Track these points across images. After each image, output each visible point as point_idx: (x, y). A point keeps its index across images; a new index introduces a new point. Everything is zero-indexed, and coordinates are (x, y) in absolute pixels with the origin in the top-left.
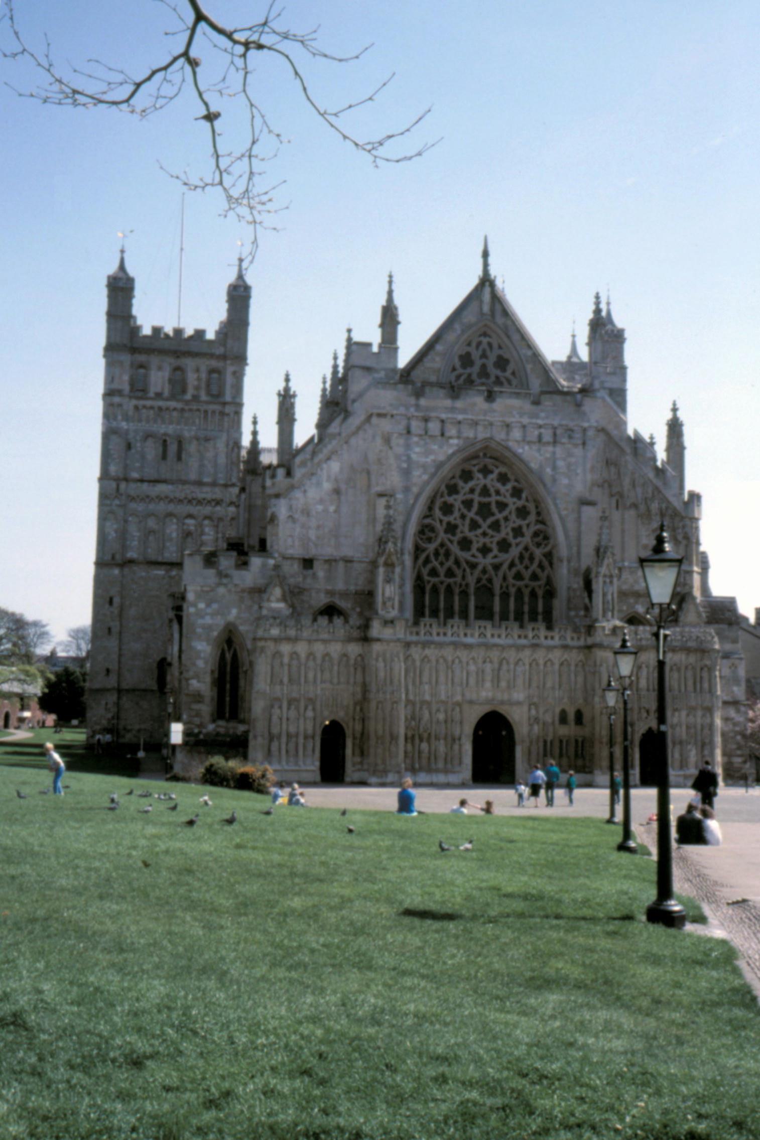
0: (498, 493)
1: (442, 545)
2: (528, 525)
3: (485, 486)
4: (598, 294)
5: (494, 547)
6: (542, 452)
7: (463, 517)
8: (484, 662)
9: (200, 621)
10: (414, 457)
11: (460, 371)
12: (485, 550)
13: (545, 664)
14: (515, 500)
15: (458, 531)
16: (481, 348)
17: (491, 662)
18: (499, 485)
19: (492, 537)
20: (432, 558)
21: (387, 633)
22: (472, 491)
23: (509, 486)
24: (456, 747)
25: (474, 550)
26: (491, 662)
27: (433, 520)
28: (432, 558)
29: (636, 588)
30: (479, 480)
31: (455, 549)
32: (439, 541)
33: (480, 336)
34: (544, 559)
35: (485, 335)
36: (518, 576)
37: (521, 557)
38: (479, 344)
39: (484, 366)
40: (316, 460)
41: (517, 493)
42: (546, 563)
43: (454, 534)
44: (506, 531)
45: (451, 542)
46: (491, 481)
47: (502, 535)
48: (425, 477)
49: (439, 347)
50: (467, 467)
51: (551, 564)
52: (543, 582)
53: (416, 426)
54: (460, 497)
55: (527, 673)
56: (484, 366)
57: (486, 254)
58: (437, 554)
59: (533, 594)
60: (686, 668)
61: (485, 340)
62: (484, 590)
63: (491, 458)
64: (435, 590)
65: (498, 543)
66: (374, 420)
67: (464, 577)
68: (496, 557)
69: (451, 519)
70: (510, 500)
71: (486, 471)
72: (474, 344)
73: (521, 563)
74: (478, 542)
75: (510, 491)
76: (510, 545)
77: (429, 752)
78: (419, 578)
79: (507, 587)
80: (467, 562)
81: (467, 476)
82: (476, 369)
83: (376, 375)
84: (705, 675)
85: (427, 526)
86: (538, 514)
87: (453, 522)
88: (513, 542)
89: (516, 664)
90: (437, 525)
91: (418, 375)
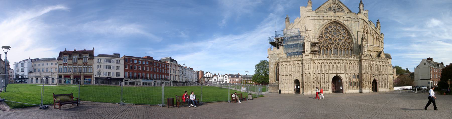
2: (346, 36)
5: (337, 40)
8: (334, 63)
12: (336, 41)
19: (337, 38)
24: (327, 85)
25: (333, 41)
26: (336, 63)
31: (328, 41)
32: (324, 39)
43: (328, 38)
45: (327, 40)
47: (340, 38)
48: (319, 27)
52: (350, 47)
54: (329, 31)
68: (338, 42)
69: (327, 35)
79: (341, 48)
80: (331, 43)
90: (323, 36)
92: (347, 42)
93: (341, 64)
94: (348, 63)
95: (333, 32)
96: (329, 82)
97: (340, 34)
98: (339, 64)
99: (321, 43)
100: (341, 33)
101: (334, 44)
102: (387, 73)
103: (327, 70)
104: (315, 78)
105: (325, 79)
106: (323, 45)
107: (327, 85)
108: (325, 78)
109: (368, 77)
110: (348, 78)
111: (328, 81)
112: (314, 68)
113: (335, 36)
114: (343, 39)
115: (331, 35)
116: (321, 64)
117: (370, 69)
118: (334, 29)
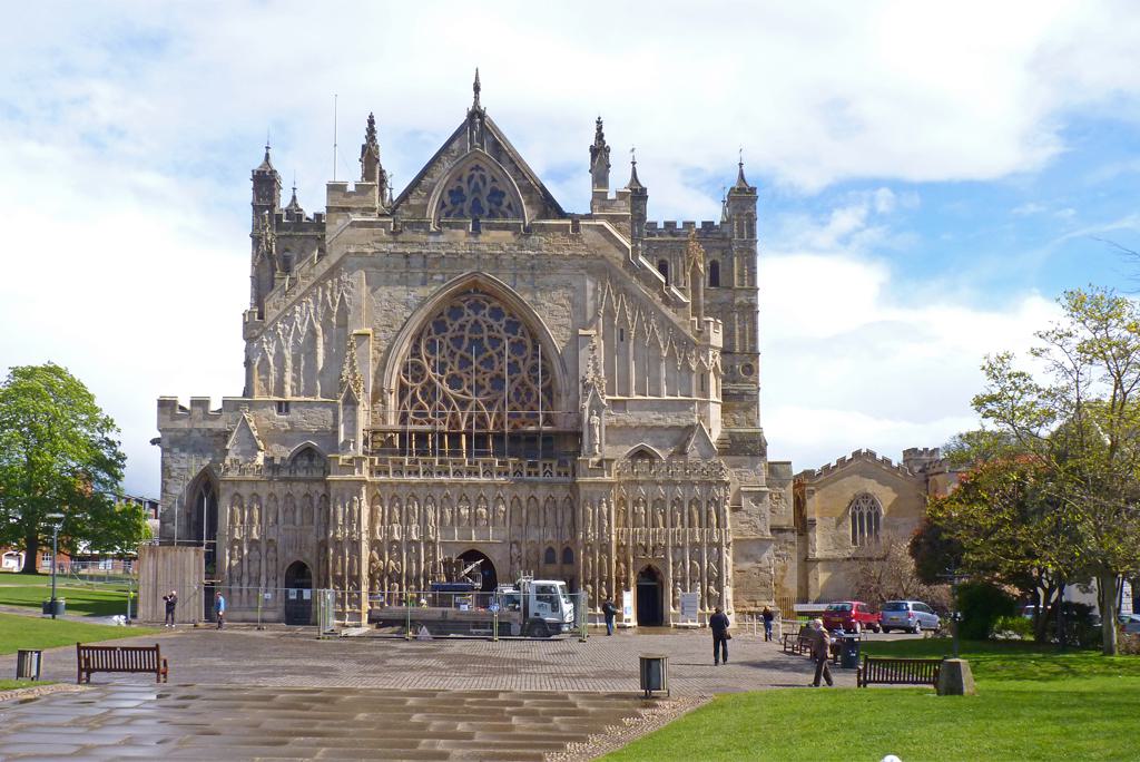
0: (490, 327)
2: (525, 360)
3: (476, 322)
5: (487, 384)
6: (536, 284)
7: (453, 354)
9: (175, 465)
11: (449, 207)
13: (528, 501)
14: (510, 335)
16: (473, 182)
18: (491, 321)
22: (462, 327)
23: (503, 322)
26: (467, 500)
30: (469, 316)
33: (472, 169)
35: (477, 168)
38: (472, 177)
41: (512, 326)
45: (441, 380)
46: (484, 316)
47: (496, 370)
50: (457, 303)
54: (449, 335)
57: (477, 88)
58: (423, 393)
61: (477, 174)
68: (489, 393)
70: (504, 335)
71: (477, 307)
72: (465, 179)
73: (517, 400)
80: (457, 400)
81: (456, 312)
82: (467, 206)
92: (528, 389)
94: (524, 499)
95: (466, 341)
97: (498, 349)
101: (469, 401)
102: (716, 540)
106: (422, 407)
108: (423, 560)
110: (520, 562)
116: (404, 501)
117: (626, 521)
118: (472, 321)
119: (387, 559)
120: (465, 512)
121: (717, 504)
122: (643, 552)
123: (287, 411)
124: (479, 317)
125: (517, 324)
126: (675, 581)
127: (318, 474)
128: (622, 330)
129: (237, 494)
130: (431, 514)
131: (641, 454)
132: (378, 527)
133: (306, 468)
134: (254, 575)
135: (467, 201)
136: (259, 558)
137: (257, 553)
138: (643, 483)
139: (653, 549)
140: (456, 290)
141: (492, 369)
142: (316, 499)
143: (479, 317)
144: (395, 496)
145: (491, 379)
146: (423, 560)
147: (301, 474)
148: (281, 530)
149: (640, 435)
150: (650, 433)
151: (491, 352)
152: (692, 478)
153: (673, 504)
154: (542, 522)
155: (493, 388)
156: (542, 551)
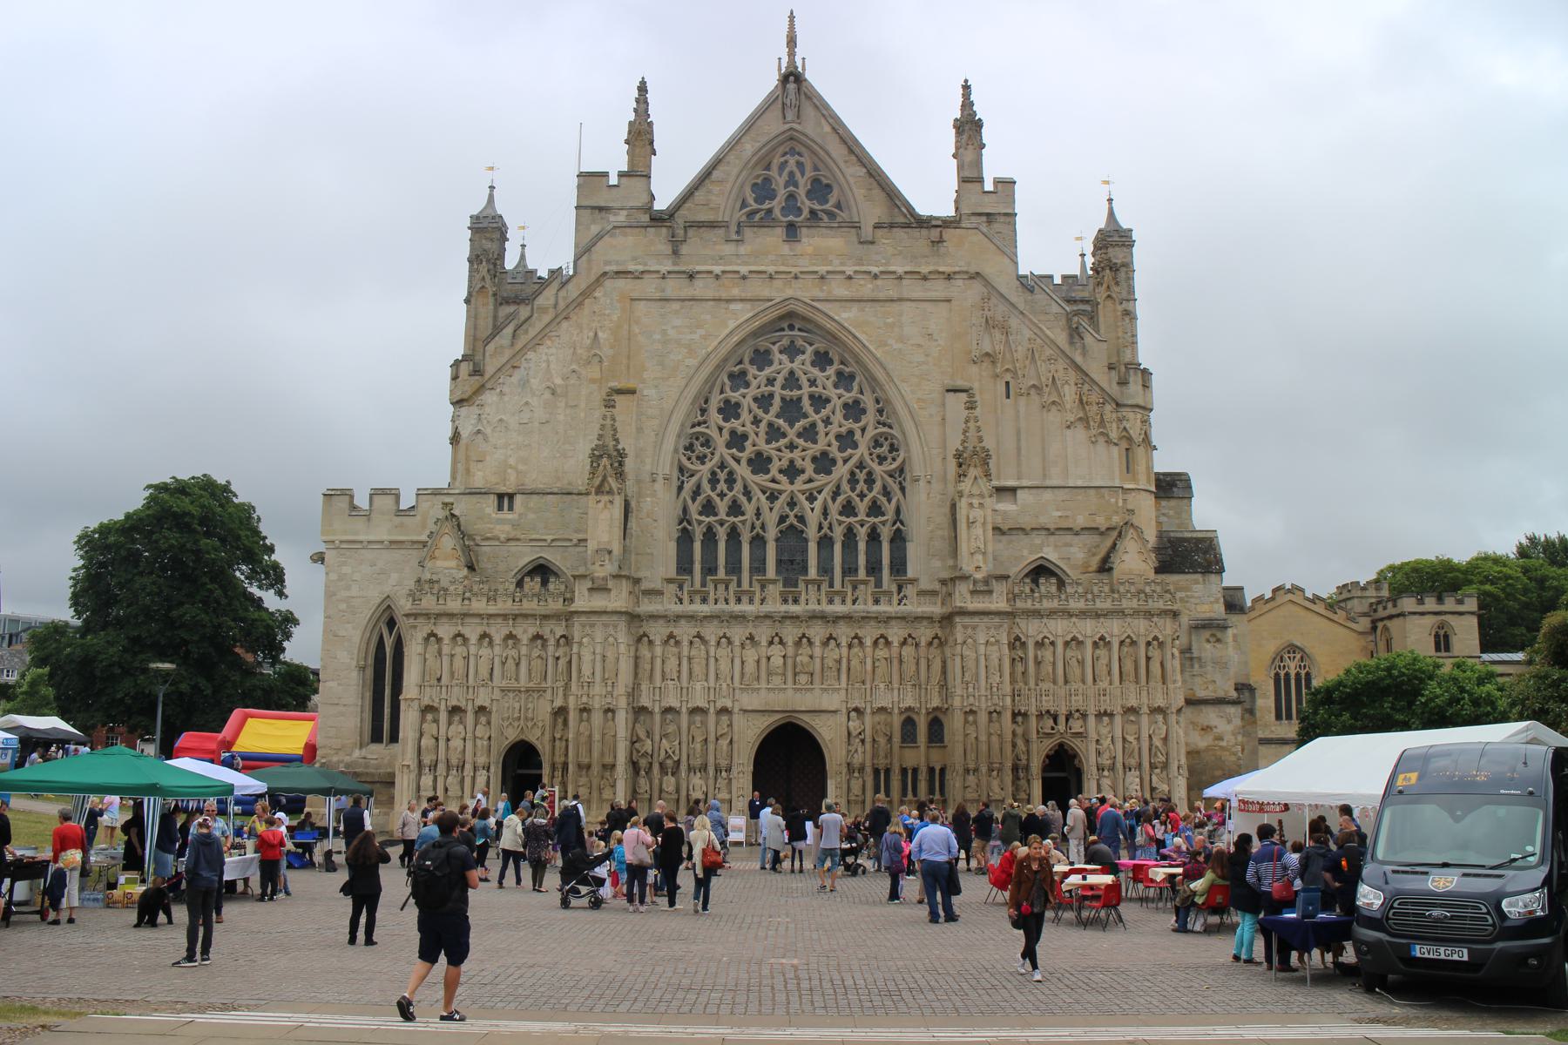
0: (813, 383)
1: (722, 466)
2: (863, 430)
3: (792, 373)
4: (966, 81)
8: (771, 643)
10: (672, 333)
12: (792, 472)
13: (876, 643)
15: (748, 444)
17: (781, 642)
18: (816, 372)
20: (706, 486)
21: (599, 602)
24: (721, 783)
25: (774, 472)
26: (781, 642)
27: (707, 427)
28: (706, 486)
29: (1043, 520)
30: (781, 364)
31: (743, 471)
32: (716, 458)
34: (890, 480)
35: (792, 152)
36: (848, 509)
37: (853, 481)
39: (791, 197)
40: (519, 346)
41: (844, 380)
42: (896, 488)
43: (742, 449)
44: (825, 441)
45: (738, 461)
46: (802, 364)
47: (821, 446)
49: (716, 175)
50: (763, 344)
51: (903, 489)
52: (890, 516)
53: (673, 287)
55: (844, 661)
56: (791, 197)
57: (792, 42)
58: (714, 481)
59: (874, 536)
60: (1122, 643)
61: (792, 161)
62: (792, 534)
63: (800, 330)
64: (710, 535)
65: (814, 459)
66: (608, 283)
67: (758, 514)
68: (810, 481)
71: (792, 351)
73: (853, 490)
74: (780, 460)
75: (833, 378)
76: (834, 462)
77: (678, 791)
78: (684, 517)
79: (830, 528)
82: (777, 204)
83: (612, 218)
84: (1155, 653)
85: (697, 436)
86: (880, 411)
87: (740, 429)
88: (839, 456)
89: (825, 644)
90: (714, 433)
91: (684, 214)
92: (870, 474)
93: (818, 651)
94: (868, 642)
95: (777, 402)
96: (735, 770)
98: (805, 650)
99: (699, 486)
100: (829, 407)
101: (780, 492)
103: (724, 686)
104: (642, 734)
105: (711, 747)
107: (721, 783)
108: (712, 738)
109: (994, 739)
110: (863, 741)
111: (723, 763)
112: (640, 671)
113: (792, 433)
114: (845, 455)
115: (763, 425)
116: (685, 643)
118: (785, 373)
119: (657, 738)
120: (777, 661)
121: (1161, 644)
122: (1051, 722)
123: (511, 508)
124: (794, 365)
125: (852, 377)
126: (1100, 769)
127: (555, 605)
128: (1007, 383)
129: (432, 634)
130: (724, 666)
131: (1040, 571)
132: (643, 687)
133: (538, 595)
134: (454, 761)
135: (778, 199)
136: (463, 734)
137: (461, 727)
138: (1052, 613)
139: (1067, 720)
140: (763, 327)
141: (815, 442)
142: (552, 642)
143: (794, 365)
144: (671, 636)
145: (814, 459)
146: (712, 738)
147: (530, 606)
148: (497, 691)
149: (1038, 541)
150: (1052, 538)
151: (814, 417)
152: (1125, 604)
153: (1095, 644)
154: (896, 677)
155: (817, 471)
156: (897, 721)
